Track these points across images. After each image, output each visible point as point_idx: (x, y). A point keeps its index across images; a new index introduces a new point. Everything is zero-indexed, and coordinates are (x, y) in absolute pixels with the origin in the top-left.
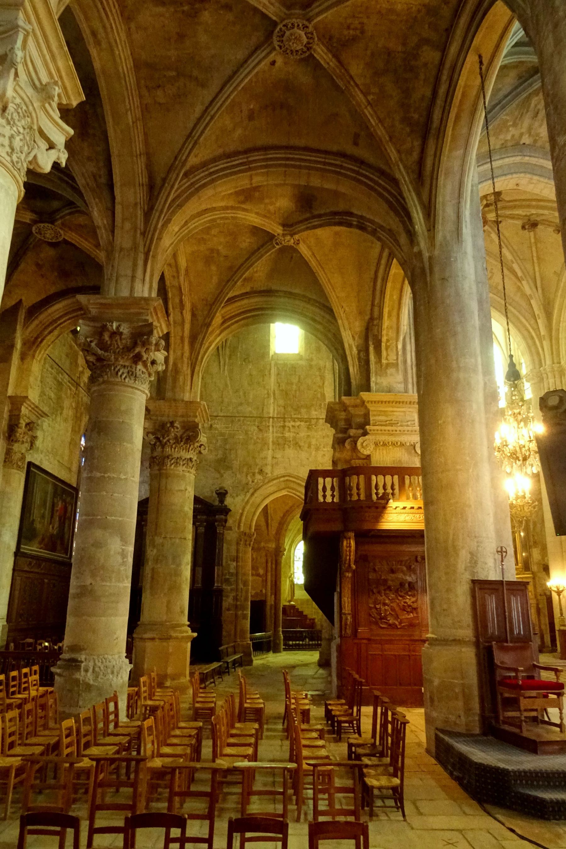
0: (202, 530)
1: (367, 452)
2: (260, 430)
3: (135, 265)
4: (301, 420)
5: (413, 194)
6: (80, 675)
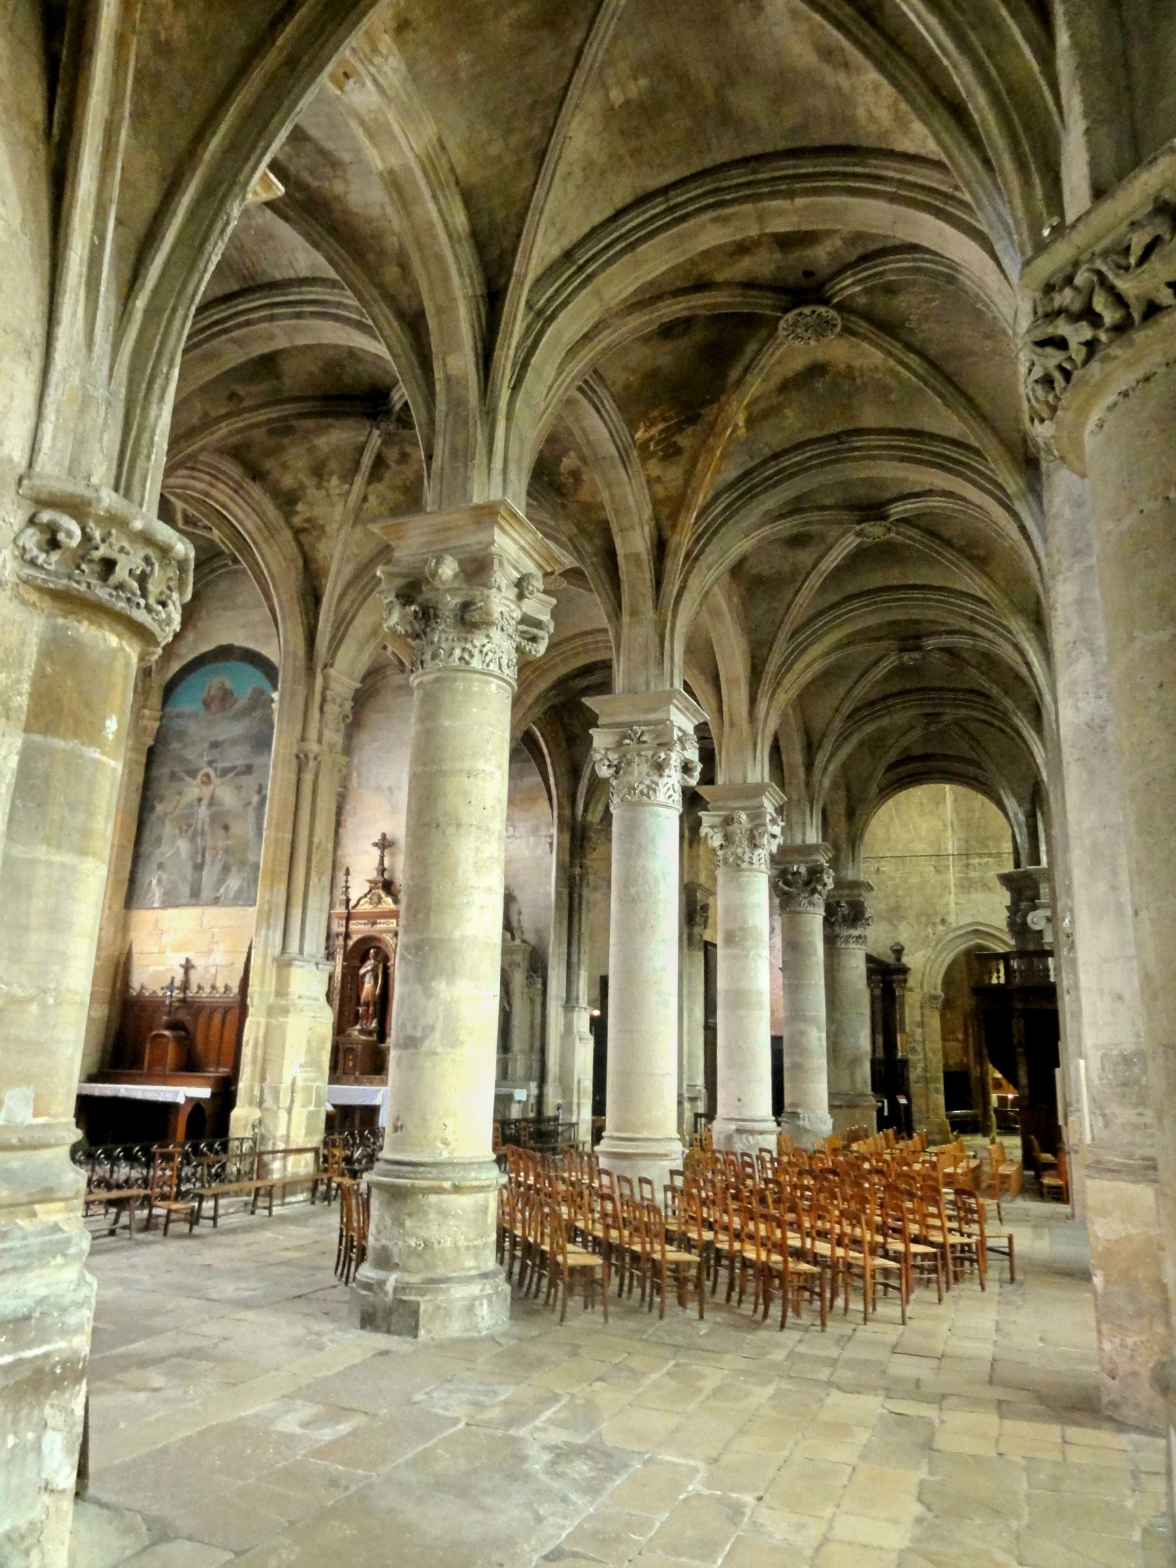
0: (878, 992)
1: (1037, 928)
2: (938, 871)
3: (804, 813)
4: (990, 855)
5: (1033, 734)
6: (801, 1123)
